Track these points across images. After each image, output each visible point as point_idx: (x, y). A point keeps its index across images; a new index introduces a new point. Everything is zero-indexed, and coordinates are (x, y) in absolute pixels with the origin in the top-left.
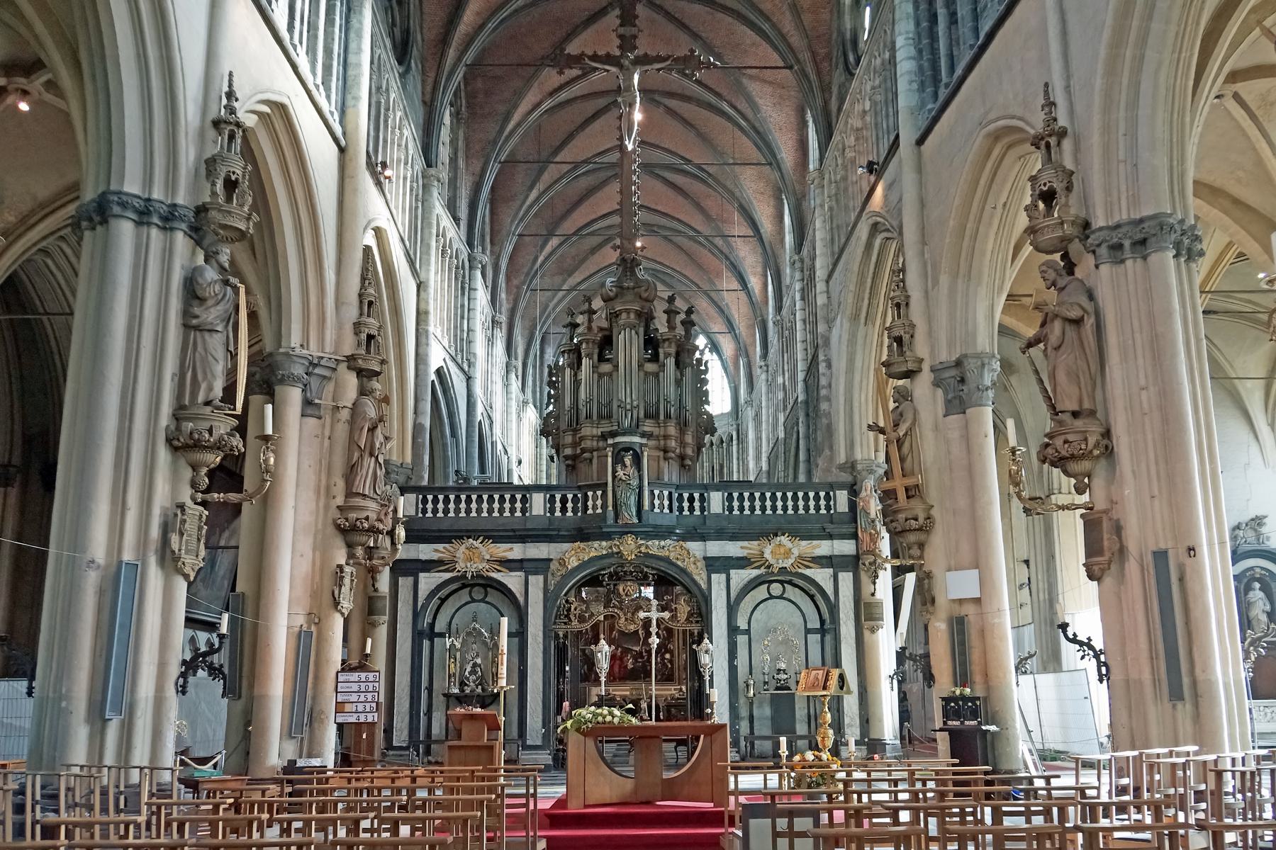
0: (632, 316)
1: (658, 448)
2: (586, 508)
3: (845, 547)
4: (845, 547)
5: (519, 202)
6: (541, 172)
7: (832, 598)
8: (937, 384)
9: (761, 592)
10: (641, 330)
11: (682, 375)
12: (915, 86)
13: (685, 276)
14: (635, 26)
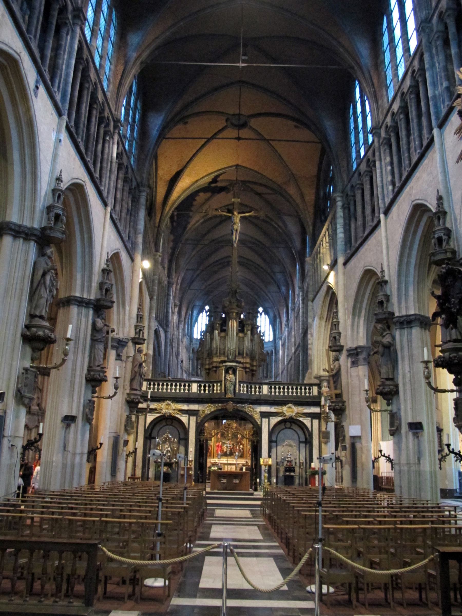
0: (234, 314)
1: (243, 368)
2: (213, 390)
3: (316, 410)
4: (316, 410)
7: (310, 429)
8: (348, 356)
9: (282, 426)
12: (343, 243)
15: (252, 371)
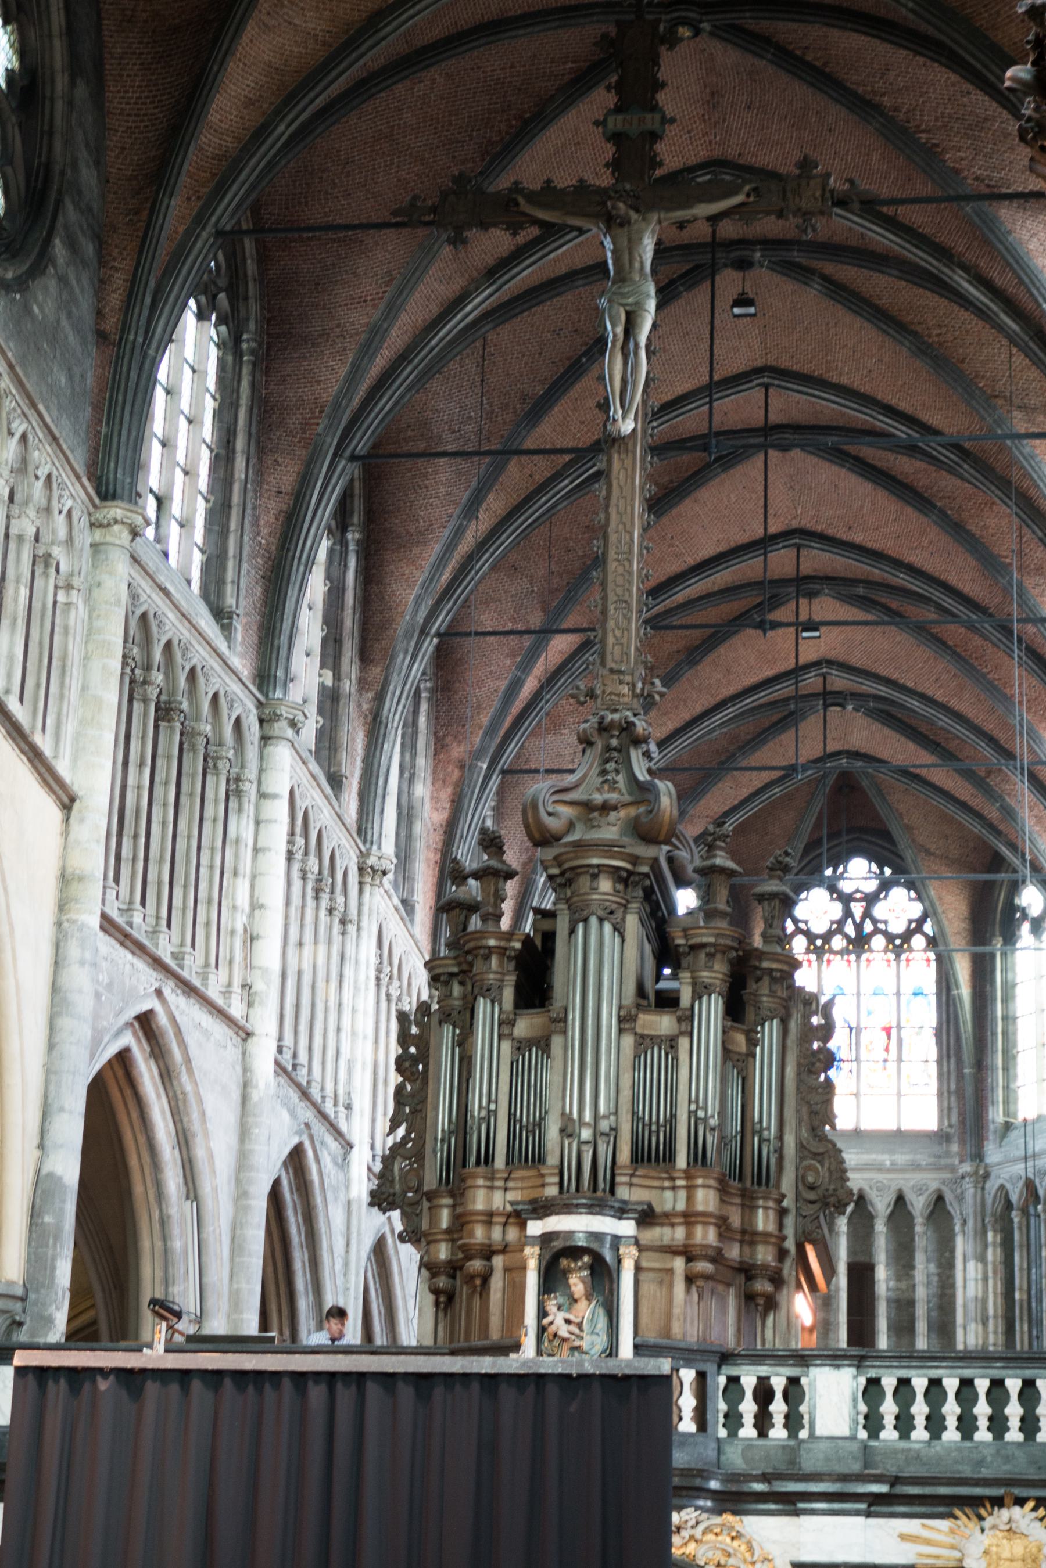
0: (605, 885)
5: (437, 548)
6: (497, 470)
10: (632, 923)
11: (753, 1043)
13: (958, 716)
14: (654, 108)
15: (747, 1271)
